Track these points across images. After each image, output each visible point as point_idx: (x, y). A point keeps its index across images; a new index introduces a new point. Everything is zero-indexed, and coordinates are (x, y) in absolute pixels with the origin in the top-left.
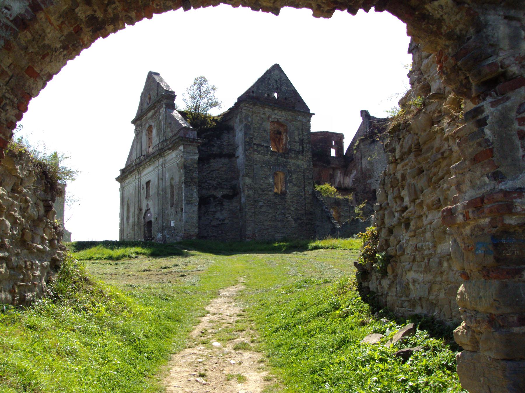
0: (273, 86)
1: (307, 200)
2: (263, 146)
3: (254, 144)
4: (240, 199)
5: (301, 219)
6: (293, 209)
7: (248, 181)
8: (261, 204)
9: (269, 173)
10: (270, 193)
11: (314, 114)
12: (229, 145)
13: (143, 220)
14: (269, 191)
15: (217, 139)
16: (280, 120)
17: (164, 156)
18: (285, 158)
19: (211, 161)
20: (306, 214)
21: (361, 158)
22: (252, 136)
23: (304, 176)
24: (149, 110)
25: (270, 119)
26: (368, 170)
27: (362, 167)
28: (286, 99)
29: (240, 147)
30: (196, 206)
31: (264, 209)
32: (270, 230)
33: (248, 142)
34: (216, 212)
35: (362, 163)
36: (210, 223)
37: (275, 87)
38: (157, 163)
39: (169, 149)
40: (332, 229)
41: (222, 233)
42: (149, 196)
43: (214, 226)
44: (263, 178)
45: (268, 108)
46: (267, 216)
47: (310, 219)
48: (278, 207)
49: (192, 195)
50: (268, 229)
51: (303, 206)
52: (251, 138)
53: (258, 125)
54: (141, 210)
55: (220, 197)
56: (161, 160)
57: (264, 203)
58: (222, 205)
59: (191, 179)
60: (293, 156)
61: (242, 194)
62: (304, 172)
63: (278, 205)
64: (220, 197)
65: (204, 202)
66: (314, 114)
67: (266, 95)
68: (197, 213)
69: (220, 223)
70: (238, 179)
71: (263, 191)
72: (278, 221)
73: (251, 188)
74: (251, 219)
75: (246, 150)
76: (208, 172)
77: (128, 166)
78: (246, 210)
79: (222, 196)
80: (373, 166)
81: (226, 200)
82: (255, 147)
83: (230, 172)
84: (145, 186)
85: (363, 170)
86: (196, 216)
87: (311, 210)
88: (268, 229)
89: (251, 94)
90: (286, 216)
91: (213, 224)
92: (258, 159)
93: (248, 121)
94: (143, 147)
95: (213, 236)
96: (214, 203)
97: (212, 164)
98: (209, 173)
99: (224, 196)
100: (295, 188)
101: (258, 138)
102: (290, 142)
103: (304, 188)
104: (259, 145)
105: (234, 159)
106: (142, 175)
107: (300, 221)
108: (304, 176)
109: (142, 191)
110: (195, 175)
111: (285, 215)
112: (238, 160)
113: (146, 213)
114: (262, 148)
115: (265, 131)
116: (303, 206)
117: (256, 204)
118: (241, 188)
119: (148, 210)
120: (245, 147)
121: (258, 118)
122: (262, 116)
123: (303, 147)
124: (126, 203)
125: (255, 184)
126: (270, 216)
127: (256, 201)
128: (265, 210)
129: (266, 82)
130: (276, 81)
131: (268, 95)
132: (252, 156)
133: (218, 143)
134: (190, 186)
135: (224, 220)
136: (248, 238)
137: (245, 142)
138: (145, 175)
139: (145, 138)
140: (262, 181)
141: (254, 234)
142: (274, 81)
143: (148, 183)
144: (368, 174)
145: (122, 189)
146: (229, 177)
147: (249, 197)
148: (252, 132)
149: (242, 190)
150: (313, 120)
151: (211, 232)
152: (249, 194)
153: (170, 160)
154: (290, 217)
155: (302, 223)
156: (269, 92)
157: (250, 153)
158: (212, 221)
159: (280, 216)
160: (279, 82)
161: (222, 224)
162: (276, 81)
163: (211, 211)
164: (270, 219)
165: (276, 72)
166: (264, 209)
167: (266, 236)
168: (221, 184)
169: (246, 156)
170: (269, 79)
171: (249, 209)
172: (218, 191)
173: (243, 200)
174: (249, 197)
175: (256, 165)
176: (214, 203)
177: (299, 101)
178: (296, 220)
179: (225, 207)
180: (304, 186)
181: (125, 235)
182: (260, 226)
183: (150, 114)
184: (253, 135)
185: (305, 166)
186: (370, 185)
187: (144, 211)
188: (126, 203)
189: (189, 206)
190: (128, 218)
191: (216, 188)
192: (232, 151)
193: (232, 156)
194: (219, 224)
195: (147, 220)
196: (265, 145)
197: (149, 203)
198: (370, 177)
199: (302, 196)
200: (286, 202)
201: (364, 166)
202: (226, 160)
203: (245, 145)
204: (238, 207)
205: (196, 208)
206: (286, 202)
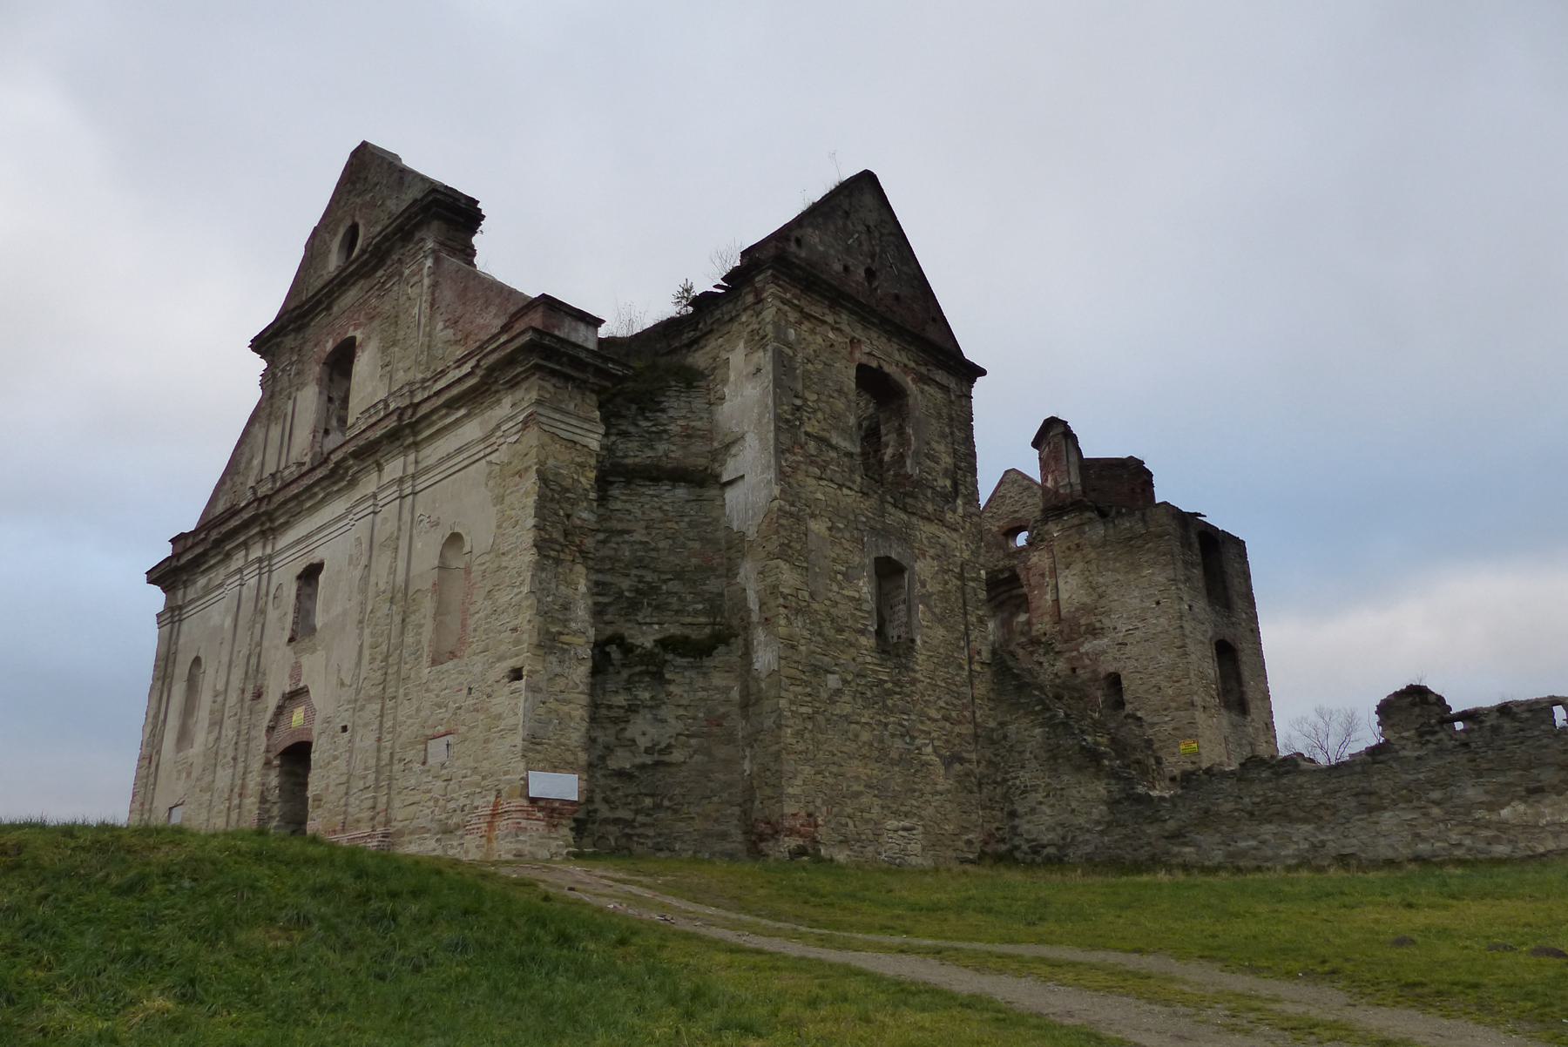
0: (860, 244)
1: (976, 682)
2: (835, 448)
3: (807, 434)
4: (747, 654)
5: (962, 760)
6: (933, 713)
7: (788, 577)
8: (833, 681)
9: (857, 559)
10: (863, 640)
11: (983, 372)
12: (689, 436)
13: (264, 739)
14: (862, 632)
15: (642, 410)
16: (887, 368)
17: (416, 445)
18: (905, 510)
19: (615, 492)
20: (976, 736)
21: (1054, 572)
22: (798, 402)
23: (962, 590)
24: (340, 283)
25: (857, 355)
26: (1084, 608)
27: (1057, 601)
28: (897, 297)
29: (748, 437)
30: (581, 660)
31: (844, 707)
32: (864, 799)
33: (787, 421)
34: (632, 709)
35: (1056, 586)
36: (602, 758)
37: (865, 248)
38: (369, 484)
39: (451, 405)
40: (1113, 804)
41: (658, 807)
42: (312, 630)
43: (621, 774)
44: (840, 577)
45: (852, 312)
46: (857, 736)
47: (990, 762)
48: (889, 703)
49: (566, 607)
50: (857, 795)
51: (965, 707)
52: (798, 408)
53: (820, 367)
54: (258, 695)
55: (649, 645)
56: (394, 467)
57: (845, 682)
58: (658, 678)
59: (566, 534)
60: (930, 507)
61: (760, 635)
62: (961, 577)
63: (889, 693)
64: (649, 645)
65: (608, 656)
66: (983, 372)
67: (838, 267)
68: (584, 700)
69: (648, 760)
70: (731, 572)
71: (840, 631)
72: (893, 763)
73: (798, 611)
74: (801, 747)
75: (780, 452)
76: (601, 536)
77: (206, 524)
78: (783, 703)
79: (659, 642)
80: (1101, 597)
81: (680, 661)
82: (812, 447)
83: (697, 545)
84: (291, 589)
85: (1064, 612)
86: (578, 712)
87: (992, 724)
88: (857, 795)
89: (793, 247)
90: (919, 742)
91: (613, 764)
92: (819, 495)
93: (789, 345)
94: (296, 433)
95: (616, 821)
96: (625, 674)
97: (618, 505)
98: (604, 542)
99: (665, 643)
100: (940, 632)
101: (820, 415)
102: (916, 453)
103: (967, 635)
104: (821, 440)
105: (713, 492)
106: (278, 547)
107: (957, 766)
108: (962, 590)
109: (272, 614)
110: (585, 515)
111: (913, 738)
112: (730, 494)
113: (280, 710)
114: (833, 454)
115: (840, 391)
116: (965, 707)
117: (814, 681)
118: (753, 604)
119: (297, 695)
120: (777, 439)
121: (819, 340)
122: (831, 335)
123: (955, 484)
124: (182, 669)
125: (812, 595)
126: (865, 736)
127: (819, 671)
128: (848, 709)
129: (840, 223)
130: (868, 227)
131: (846, 268)
132: (800, 476)
133: (644, 424)
134: (558, 562)
135: (668, 749)
136: (792, 832)
137: (778, 418)
138: (298, 542)
139: (308, 401)
140: (835, 588)
141: (810, 815)
142: (861, 228)
143: (310, 575)
144: (1083, 621)
145: (171, 617)
146: (694, 561)
147: (793, 647)
148: (799, 387)
149: (755, 618)
150: (980, 387)
151: (606, 800)
152: (790, 637)
153: (449, 457)
154: (929, 749)
155: (967, 775)
156: (850, 262)
157: (795, 470)
158: (609, 749)
159: (899, 743)
160: (877, 234)
161: (657, 764)
162: (868, 227)
163: (610, 707)
164: (864, 751)
165: (869, 199)
166: (844, 707)
167: (851, 824)
168: (654, 589)
169: (782, 475)
170: (847, 214)
171: (792, 702)
172: (640, 618)
173: (765, 658)
174: (793, 647)
175: (813, 516)
176: (625, 674)
177: (934, 320)
178: (948, 762)
179: (672, 688)
180: (967, 628)
181: (161, 804)
182: (831, 781)
183: (351, 295)
184: (805, 400)
185: (966, 555)
186: (1095, 661)
187: (272, 701)
188: (182, 669)
189: (552, 658)
190: (184, 736)
191: (632, 607)
192: (702, 462)
193: (703, 479)
194: (643, 767)
195: (284, 740)
196: (845, 444)
197: (306, 660)
198: (1094, 632)
199: (961, 667)
200: (914, 682)
201: (1064, 596)
202: (681, 492)
203: (778, 429)
204: (735, 695)
205: (580, 673)
206: (914, 682)
